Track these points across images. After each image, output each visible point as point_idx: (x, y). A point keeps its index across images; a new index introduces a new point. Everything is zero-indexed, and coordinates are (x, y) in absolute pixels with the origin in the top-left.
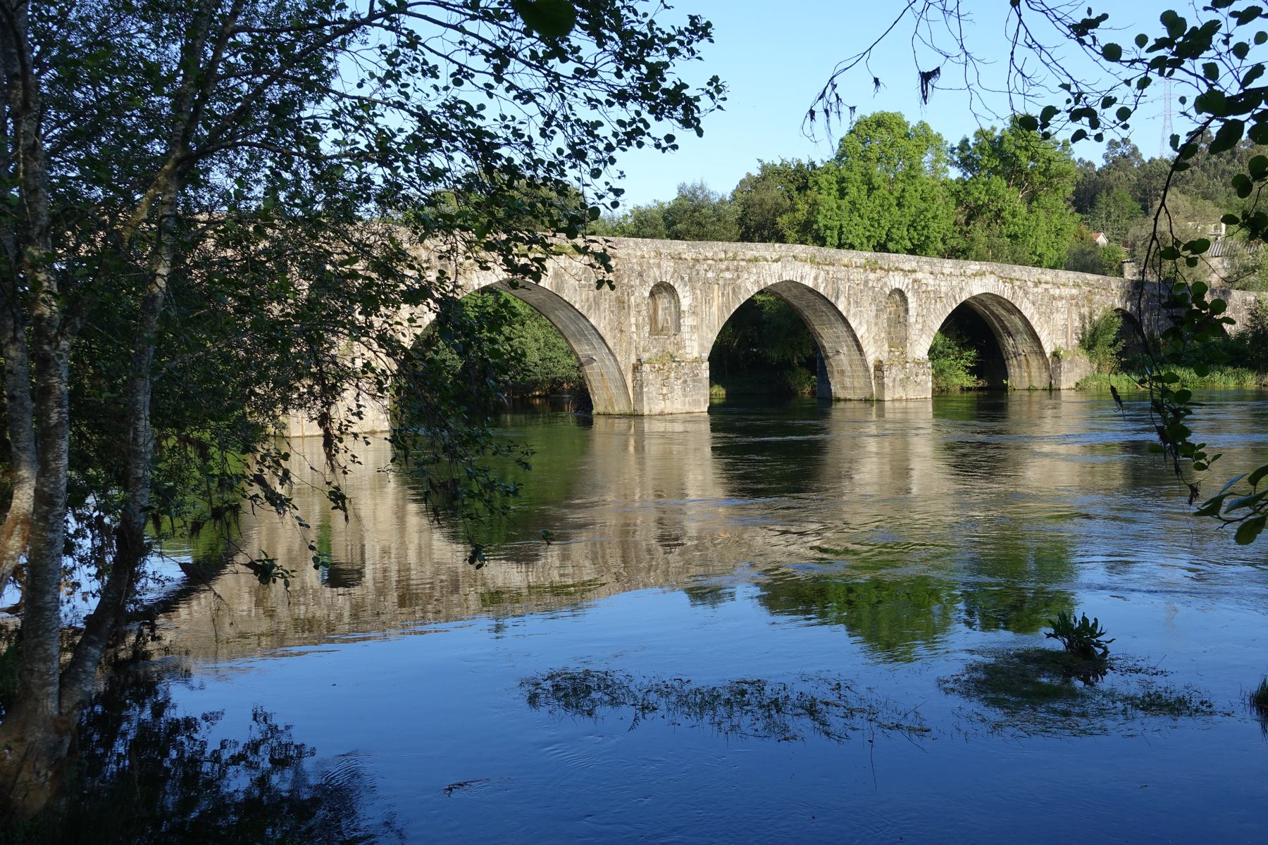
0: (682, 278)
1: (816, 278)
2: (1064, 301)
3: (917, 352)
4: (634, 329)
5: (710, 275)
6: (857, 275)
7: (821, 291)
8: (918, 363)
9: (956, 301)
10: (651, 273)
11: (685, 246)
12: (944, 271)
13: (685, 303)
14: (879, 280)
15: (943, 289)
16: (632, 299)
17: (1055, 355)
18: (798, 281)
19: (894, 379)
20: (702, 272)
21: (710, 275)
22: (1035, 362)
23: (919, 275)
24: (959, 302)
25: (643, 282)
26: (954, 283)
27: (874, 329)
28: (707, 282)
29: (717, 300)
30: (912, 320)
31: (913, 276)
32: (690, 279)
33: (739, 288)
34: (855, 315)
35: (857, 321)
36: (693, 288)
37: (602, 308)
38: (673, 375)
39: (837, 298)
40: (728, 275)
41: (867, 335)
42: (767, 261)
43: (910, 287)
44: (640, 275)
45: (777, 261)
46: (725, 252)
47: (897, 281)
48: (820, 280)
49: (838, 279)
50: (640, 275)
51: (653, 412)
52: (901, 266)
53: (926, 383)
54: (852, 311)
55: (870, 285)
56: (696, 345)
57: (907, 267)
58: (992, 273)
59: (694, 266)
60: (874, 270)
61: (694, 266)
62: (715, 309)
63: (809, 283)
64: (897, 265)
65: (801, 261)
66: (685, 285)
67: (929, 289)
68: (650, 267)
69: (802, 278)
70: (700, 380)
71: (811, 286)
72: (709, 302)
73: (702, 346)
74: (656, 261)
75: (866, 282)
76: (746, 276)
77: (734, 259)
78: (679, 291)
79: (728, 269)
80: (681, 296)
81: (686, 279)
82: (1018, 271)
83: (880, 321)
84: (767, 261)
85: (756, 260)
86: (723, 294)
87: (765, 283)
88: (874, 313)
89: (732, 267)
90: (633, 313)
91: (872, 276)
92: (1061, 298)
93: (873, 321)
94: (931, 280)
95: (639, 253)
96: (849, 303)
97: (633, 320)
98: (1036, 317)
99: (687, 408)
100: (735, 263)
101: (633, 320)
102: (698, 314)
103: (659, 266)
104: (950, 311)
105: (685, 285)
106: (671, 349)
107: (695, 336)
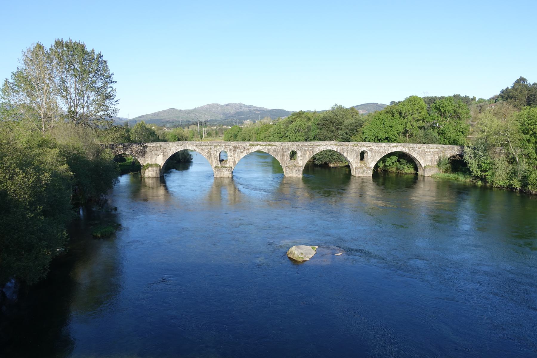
0: (299, 150)
1: (337, 149)
2: (431, 153)
3: (371, 165)
4: (286, 160)
5: (306, 149)
6: (350, 148)
7: (339, 151)
8: (370, 168)
9: (386, 153)
10: (291, 149)
11: (300, 143)
12: (382, 146)
14: (357, 149)
15: (381, 150)
16: (286, 154)
17: (425, 167)
18: (332, 149)
19: (359, 172)
20: (304, 148)
21: (306, 149)
23: (373, 147)
24: (387, 153)
25: (289, 151)
26: (385, 149)
27: (356, 160)
28: (305, 150)
29: (308, 153)
31: (370, 147)
32: (301, 150)
33: (314, 151)
34: (349, 157)
35: (350, 158)
36: (301, 151)
37: (278, 156)
38: (293, 169)
39: (344, 153)
40: (311, 149)
41: (353, 161)
42: (322, 145)
43: (369, 150)
44: (288, 149)
45: (325, 145)
46: (311, 144)
47: (364, 149)
48: (338, 149)
49: (344, 149)
50: (288, 149)
51: (288, 176)
52: (366, 145)
53: (370, 173)
54: (348, 156)
55: (355, 150)
57: (368, 145)
58: (401, 146)
59: (302, 147)
60: (356, 146)
61: (302, 147)
62: (307, 156)
63: (335, 150)
64: (364, 145)
65: (333, 145)
66: (299, 151)
67: (376, 150)
68: (290, 147)
69: (333, 149)
70: (300, 171)
71: (335, 150)
72: (306, 154)
73: (303, 163)
74: (292, 146)
75: (353, 149)
76: (316, 149)
77: (313, 145)
79: (311, 147)
81: (300, 150)
82: (411, 145)
83: (357, 158)
84: (322, 145)
85: (319, 145)
86: (309, 153)
87: (321, 150)
88: (356, 156)
89: (312, 147)
91: (355, 148)
92: (430, 152)
93: (355, 158)
94: (377, 148)
95: (288, 145)
96: (348, 154)
97: (286, 158)
98: (418, 157)
99: (297, 176)
100: (313, 146)
101: (286, 158)
102: (302, 157)
103: (293, 147)
104: (384, 156)
106: (295, 164)
107: (302, 161)
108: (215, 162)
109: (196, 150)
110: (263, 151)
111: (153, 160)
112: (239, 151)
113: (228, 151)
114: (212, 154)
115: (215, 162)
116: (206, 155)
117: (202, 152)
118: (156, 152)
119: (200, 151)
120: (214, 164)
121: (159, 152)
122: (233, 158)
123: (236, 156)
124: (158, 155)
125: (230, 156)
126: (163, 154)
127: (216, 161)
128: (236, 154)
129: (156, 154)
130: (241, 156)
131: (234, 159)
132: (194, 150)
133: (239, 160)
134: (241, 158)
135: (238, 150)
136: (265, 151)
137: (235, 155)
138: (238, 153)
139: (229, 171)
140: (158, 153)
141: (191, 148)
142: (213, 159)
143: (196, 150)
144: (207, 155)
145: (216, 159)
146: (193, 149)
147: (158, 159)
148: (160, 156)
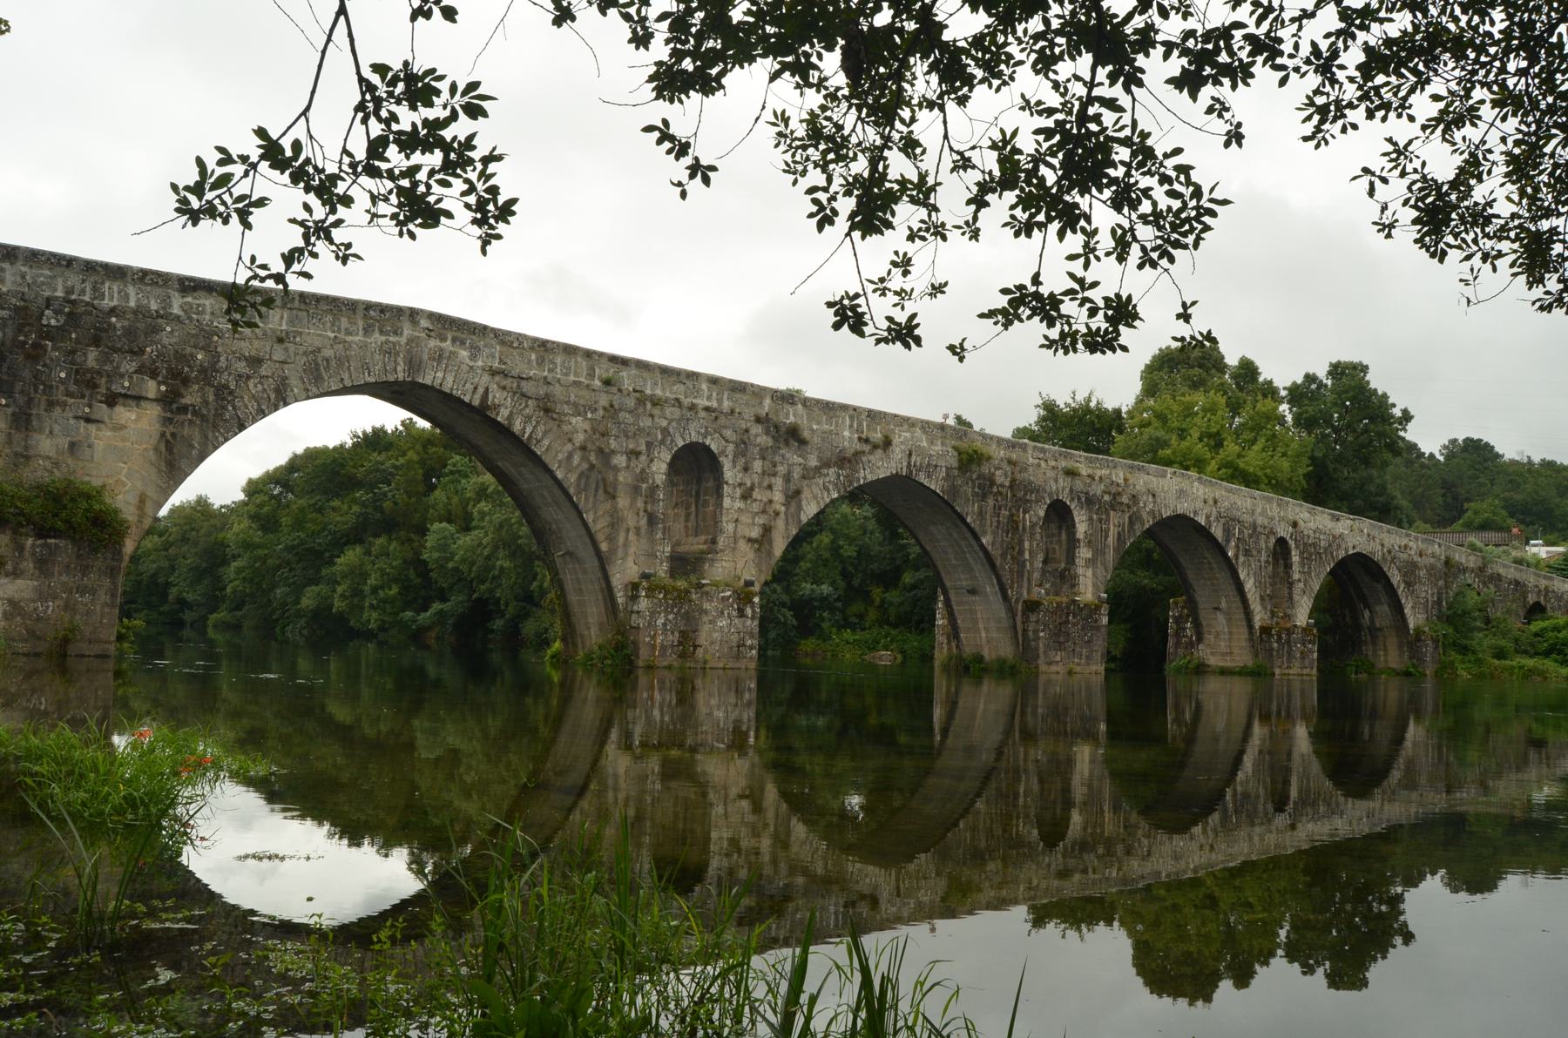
13: (1081, 529)
22: (1392, 642)
30: (1296, 576)
35: (1245, 572)
39: (1228, 541)
54: (1242, 559)
56: (1090, 583)
66: (1082, 508)
78: (1075, 513)
80: (1077, 520)
90: (1026, 537)
105: (1082, 508)
108: (638, 529)
109: (496, 407)
110: (926, 482)
111: (46, 445)
112: (797, 459)
113: (731, 447)
114: (620, 460)
115: (632, 537)
116: (570, 456)
117: (541, 429)
118: (92, 357)
119: (528, 418)
120: (626, 545)
121: (129, 366)
122: (756, 507)
123: (778, 497)
124: (112, 400)
125: (738, 492)
126: (168, 401)
127: (644, 522)
128: (778, 482)
129: (93, 386)
130: (804, 503)
131: (760, 520)
132: (476, 402)
133: (794, 532)
134: (804, 519)
135: (788, 455)
136: (933, 487)
137: (770, 487)
138: (787, 478)
139: (741, 614)
140: (115, 375)
141: (450, 379)
142: (623, 502)
143: (496, 407)
144: (576, 459)
145: (640, 504)
146: (469, 387)
147: (101, 439)
148: (125, 414)
